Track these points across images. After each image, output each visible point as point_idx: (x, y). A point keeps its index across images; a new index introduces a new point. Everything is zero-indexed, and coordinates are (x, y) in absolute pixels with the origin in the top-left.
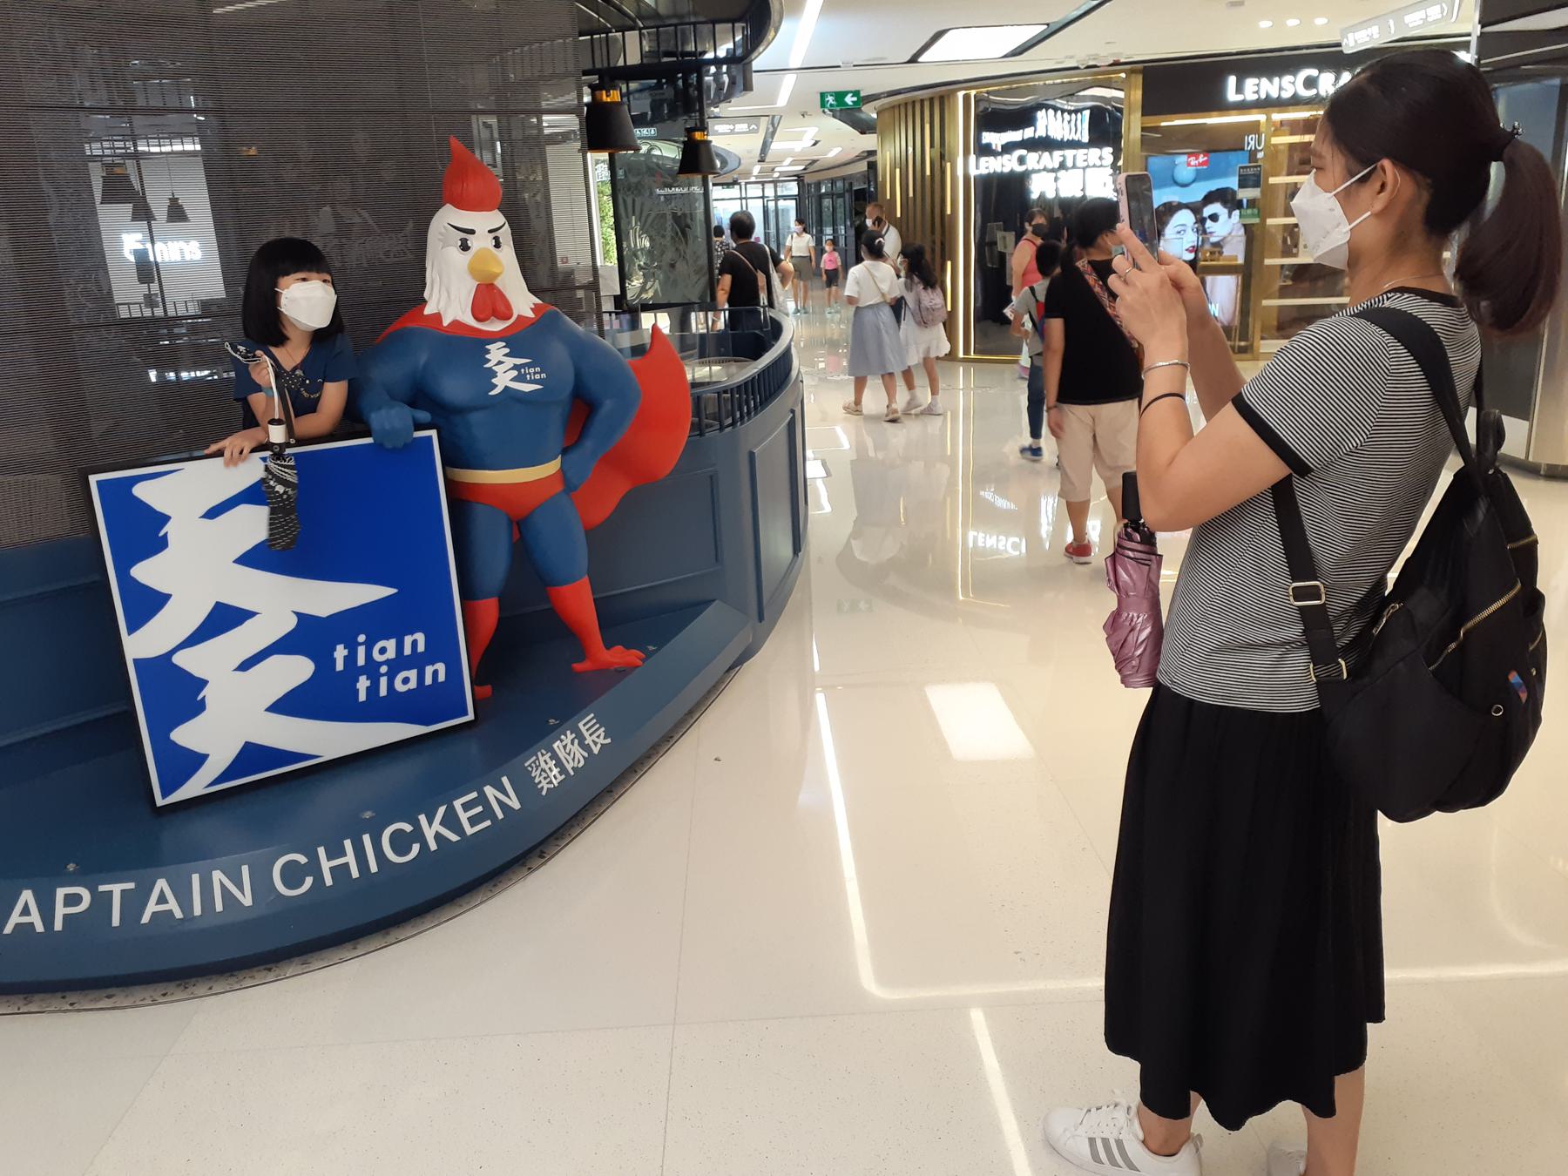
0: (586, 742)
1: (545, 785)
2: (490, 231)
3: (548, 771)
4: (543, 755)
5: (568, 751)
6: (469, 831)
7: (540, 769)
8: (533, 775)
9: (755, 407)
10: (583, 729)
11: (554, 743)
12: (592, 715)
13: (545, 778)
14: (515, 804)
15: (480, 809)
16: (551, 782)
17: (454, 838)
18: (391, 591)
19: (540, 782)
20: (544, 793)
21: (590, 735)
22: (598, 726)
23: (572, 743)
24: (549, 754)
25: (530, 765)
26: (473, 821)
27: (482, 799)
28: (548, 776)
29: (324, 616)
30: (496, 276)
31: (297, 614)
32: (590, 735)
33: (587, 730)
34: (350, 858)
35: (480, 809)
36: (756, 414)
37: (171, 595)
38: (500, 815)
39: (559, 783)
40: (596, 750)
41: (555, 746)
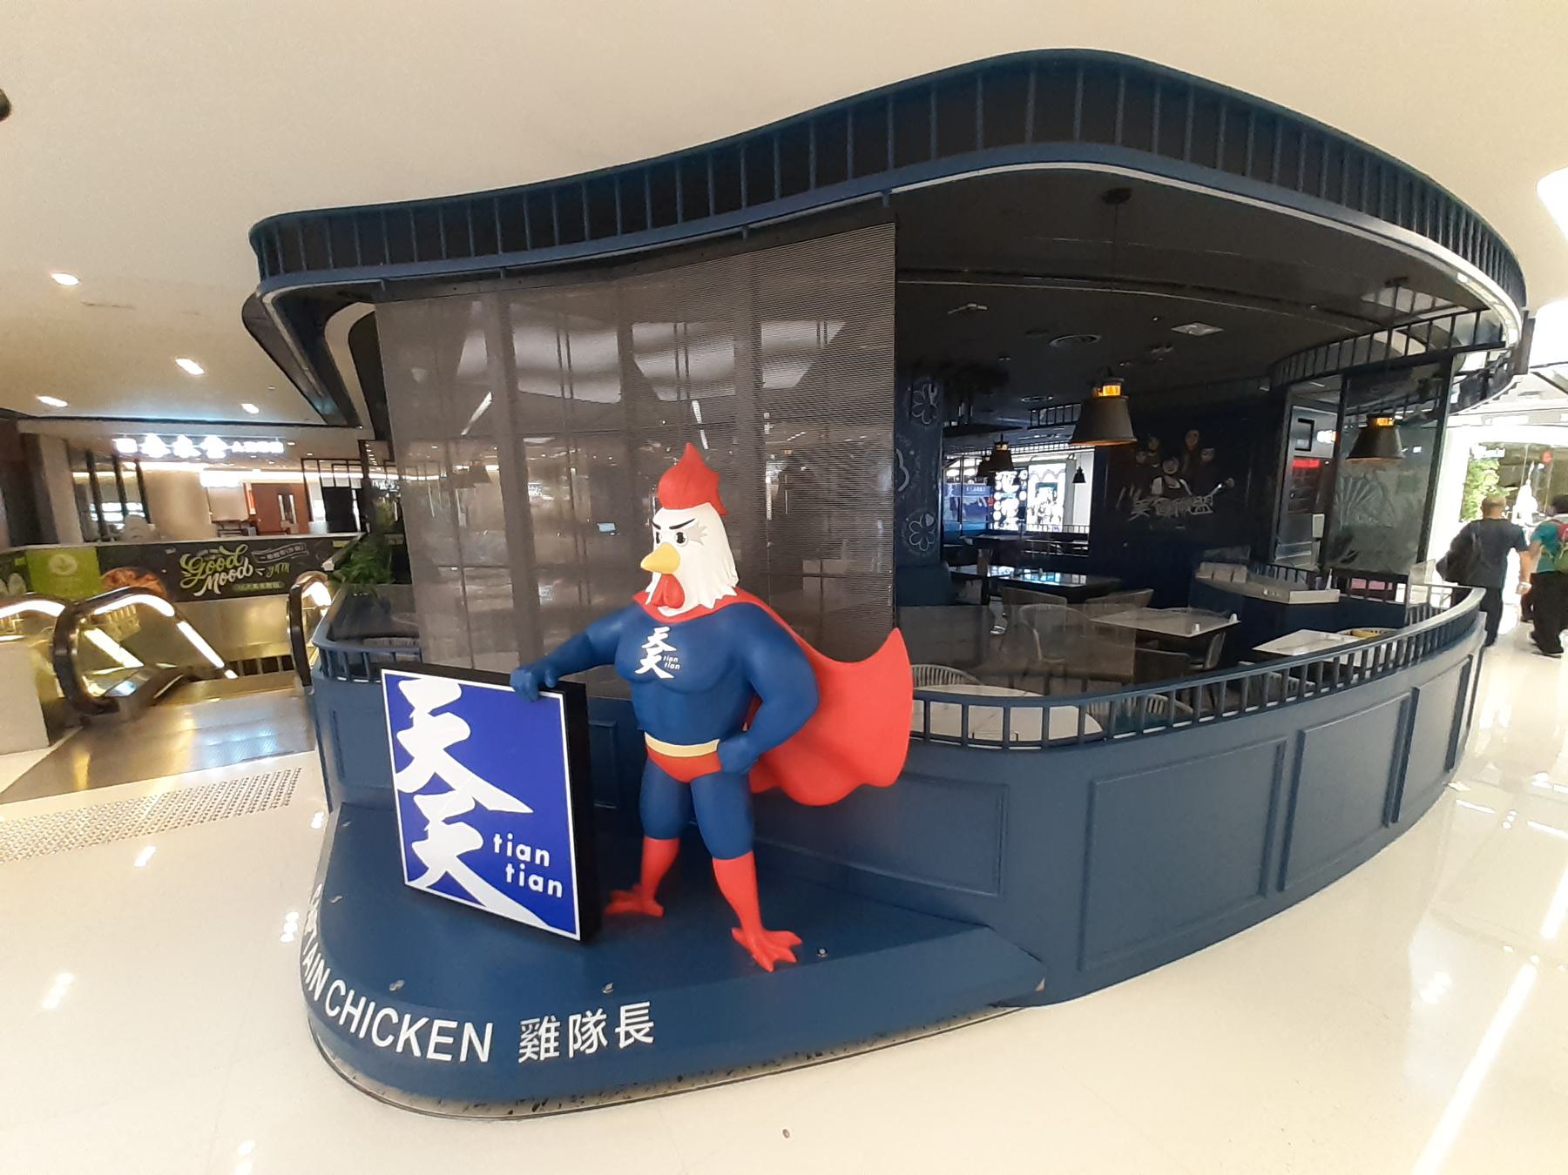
0: (617, 1030)
1: (529, 1053)
2: (672, 528)
3: (543, 1040)
4: (549, 1021)
5: (583, 1030)
6: (431, 1055)
7: (535, 1033)
8: (523, 1037)
9: (1416, 657)
10: (623, 1015)
11: (573, 1014)
12: (648, 1004)
13: (533, 1046)
14: (484, 1056)
15: (450, 1040)
16: (538, 1053)
17: (417, 1052)
18: (527, 810)
19: (526, 1047)
20: (521, 1060)
21: (627, 1025)
22: (647, 1018)
23: (596, 1024)
24: (558, 1024)
25: (527, 1026)
26: (440, 1048)
27: (457, 1034)
28: (539, 1046)
29: (490, 808)
30: (676, 569)
31: (477, 803)
32: (627, 1025)
33: (627, 1018)
34: (357, 1013)
35: (450, 1040)
36: (1415, 664)
37: (449, 750)
38: (463, 1058)
39: (546, 1059)
40: (623, 1044)
41: (572, 1018)
